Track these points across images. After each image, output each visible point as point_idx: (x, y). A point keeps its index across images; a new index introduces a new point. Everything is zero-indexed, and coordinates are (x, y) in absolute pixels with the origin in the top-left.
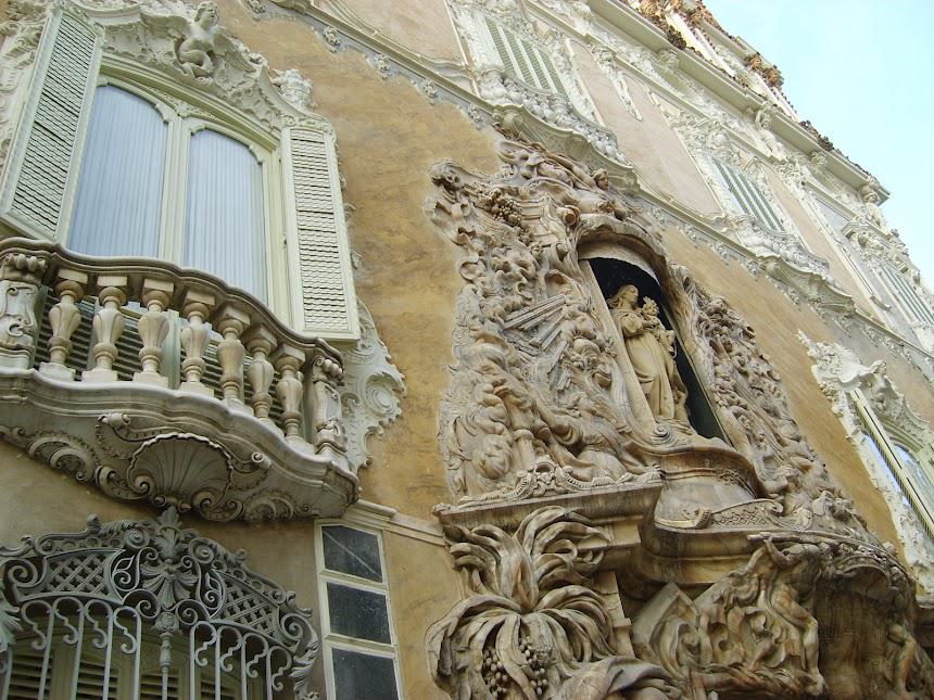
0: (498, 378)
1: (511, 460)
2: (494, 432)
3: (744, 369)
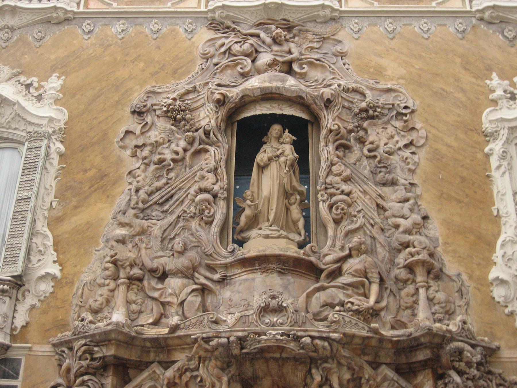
0: (112, 253)
1: (108, 301)
2: (104, 285)
3: (372, 154)
